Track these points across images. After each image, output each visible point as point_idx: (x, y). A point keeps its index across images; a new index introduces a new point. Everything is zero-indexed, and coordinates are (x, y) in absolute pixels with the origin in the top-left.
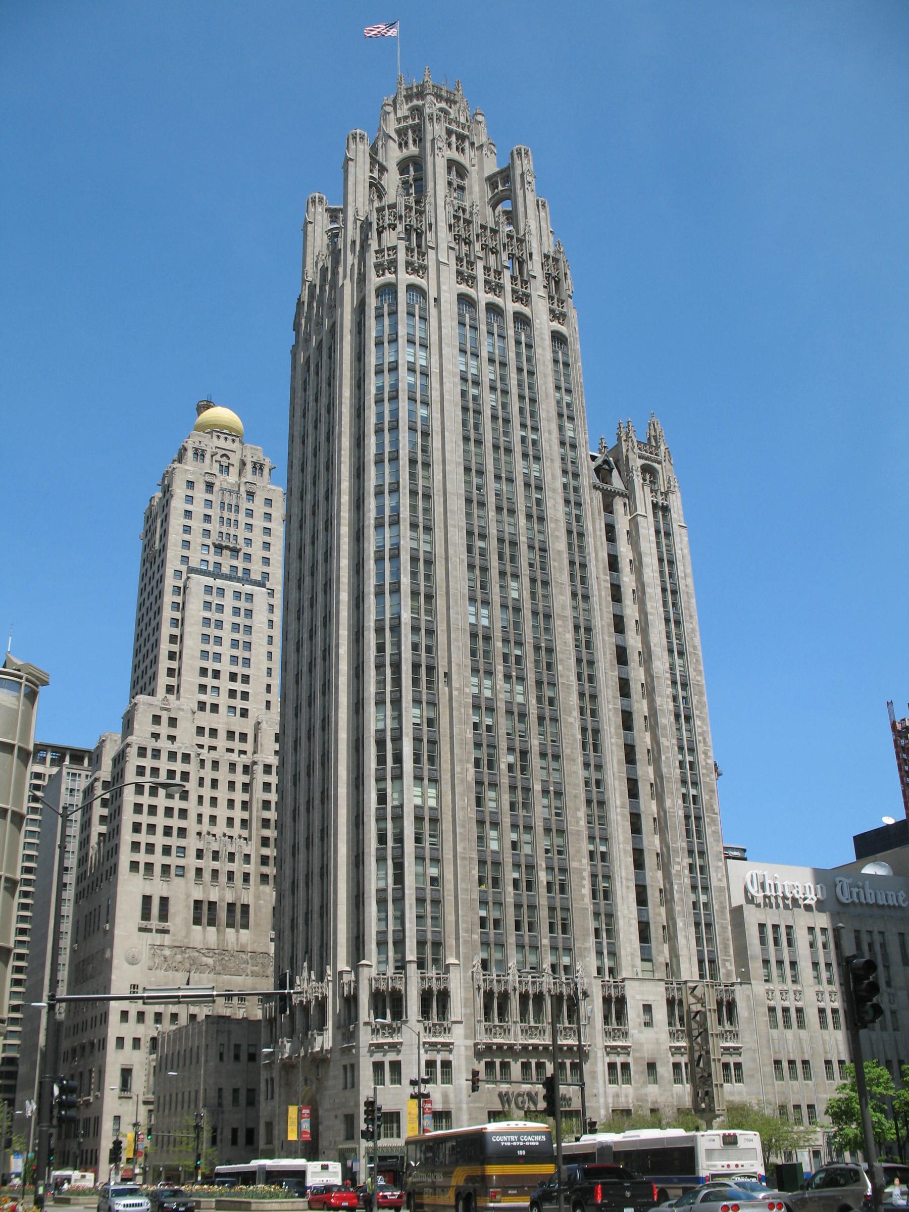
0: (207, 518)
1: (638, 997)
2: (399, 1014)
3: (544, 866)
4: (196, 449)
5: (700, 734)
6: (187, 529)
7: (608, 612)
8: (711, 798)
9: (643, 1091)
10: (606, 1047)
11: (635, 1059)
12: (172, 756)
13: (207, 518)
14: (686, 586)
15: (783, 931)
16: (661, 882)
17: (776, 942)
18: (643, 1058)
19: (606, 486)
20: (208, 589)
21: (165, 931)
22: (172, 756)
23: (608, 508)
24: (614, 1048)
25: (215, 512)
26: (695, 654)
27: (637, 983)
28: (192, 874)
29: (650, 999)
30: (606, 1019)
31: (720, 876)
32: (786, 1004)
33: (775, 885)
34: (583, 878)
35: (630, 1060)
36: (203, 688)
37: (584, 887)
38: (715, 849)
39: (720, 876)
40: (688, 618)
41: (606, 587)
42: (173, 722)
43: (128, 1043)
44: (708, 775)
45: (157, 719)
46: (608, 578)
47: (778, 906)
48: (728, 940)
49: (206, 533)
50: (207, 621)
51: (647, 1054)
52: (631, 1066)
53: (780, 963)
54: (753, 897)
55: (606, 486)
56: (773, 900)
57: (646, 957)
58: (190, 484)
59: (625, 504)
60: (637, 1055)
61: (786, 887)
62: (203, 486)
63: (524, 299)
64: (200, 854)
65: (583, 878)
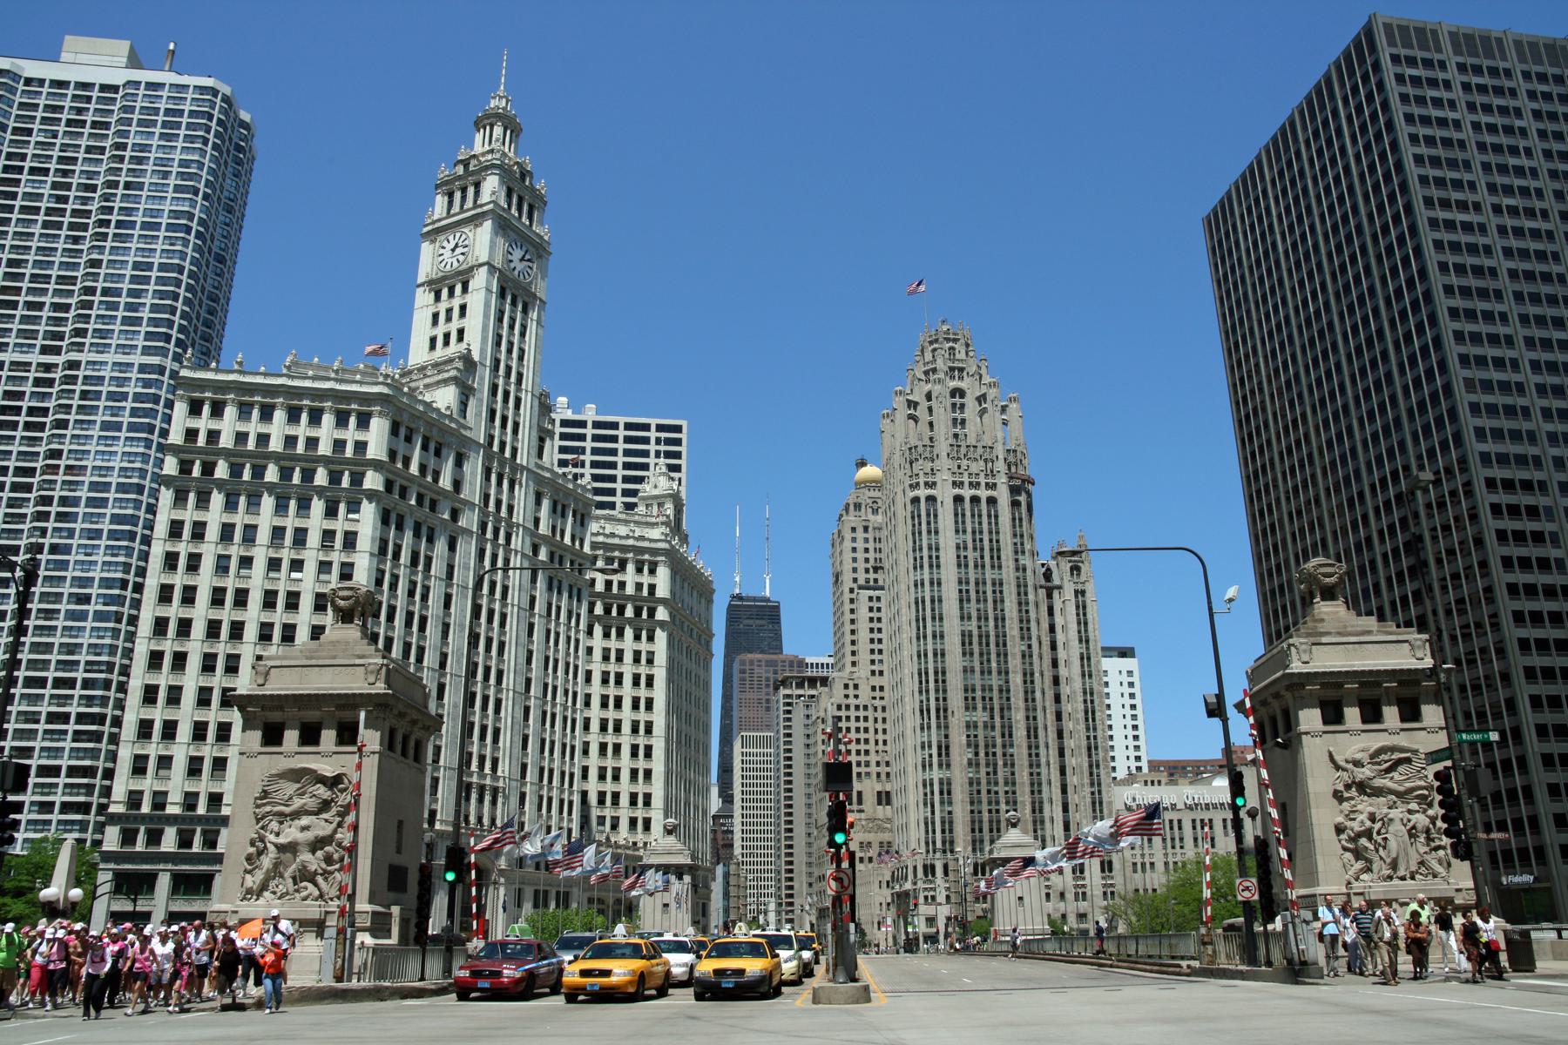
0: (867, 550)
2: (934, 874)
6: (855, 560)
12: (857, 707)
13: (867, 550)
20: (871, 599)
21: (861, 811)
22: (857, 707)
23: (1050, 596)
25: (871, 545)
28: (874, 776)
36: (873, 662)
42: (856, 687)
45: (846, 686)
49: (867, 560)
50: (871, 620)
51: (1060, 888)
58: (854, 530)
63: (993, 486)
64: (878, 764)
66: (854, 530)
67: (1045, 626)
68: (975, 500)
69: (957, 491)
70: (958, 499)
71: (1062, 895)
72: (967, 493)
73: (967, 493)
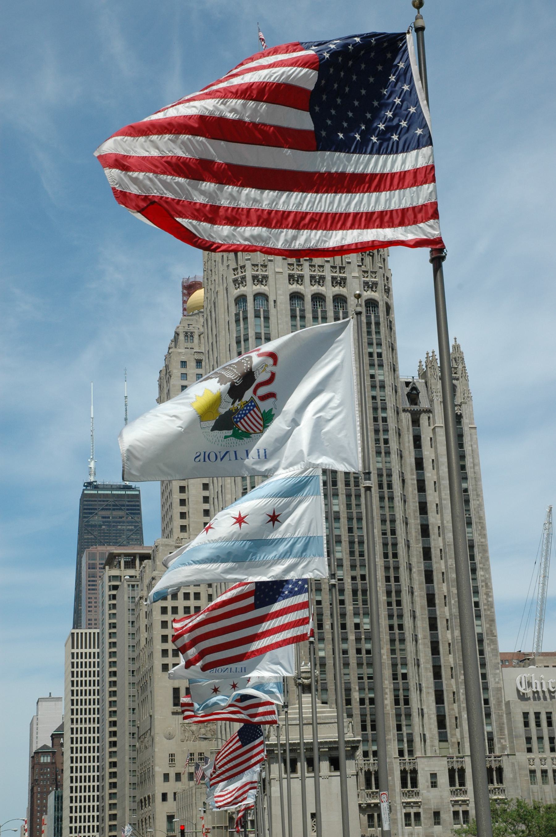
1: (427, 769)
3: (357, 688)
4: (186, 333)
5: (482, 581)
7: (413, 502)
8: (491, 626)
9: (430, 830)
10: (403, 803)
11: (424, 810)
14: (475, 473)
15: (543, 717)
16: (454, 687)
17: (538, 724)
18: (431, 809)
19: (415, 408)
23: (416, 422)
24: (409, 803)
26: (480, 523)
27: (425, 760)
29: (435, 770)
30: (404, 784)
31: (497, 680)
32: (545, 767)
33: (541, 684)
34: (386, 694)
35: (421, 810)
37: (386, 699)
38: (493, 661)
39: (497, 680)
40: (475, 497)
41: (412, 484)
43: (170, 797)
44: (489, 610)
46: (415, 477)
47: (545, 699)
48: (503, 724)
51: (433, 806)
52: (422, 814)
53: (540, 739)
54: (524, 694)
55: (415, 408)
56: (541, 695)
57: (443, 739)
58: (184, 364)
59: (429, 418)
60: (426, 807)
61: (550, 684)
62: (194, 364)
63: (342, 282)
65: (386, 694)
66: (184, 364)
67: (410, 460)
68: (318, 298)
69: (295, 287)
70: (296, 297)
71: (437, 814)
72: (308, 290)
73: (308, 290)
